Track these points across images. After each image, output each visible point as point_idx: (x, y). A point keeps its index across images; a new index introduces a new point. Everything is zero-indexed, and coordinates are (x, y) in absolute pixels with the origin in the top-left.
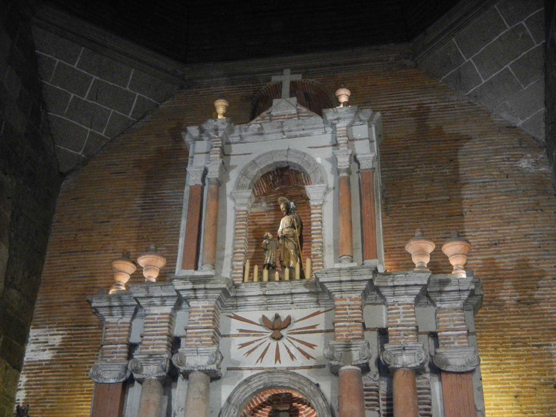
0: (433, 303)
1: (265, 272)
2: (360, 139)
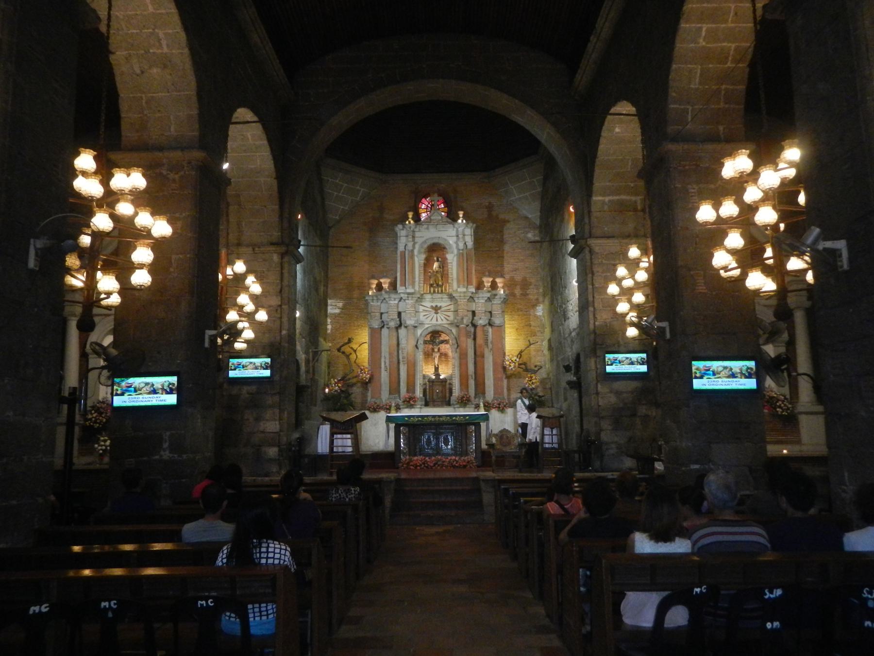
1: (432, 289)
2: (467, 235)
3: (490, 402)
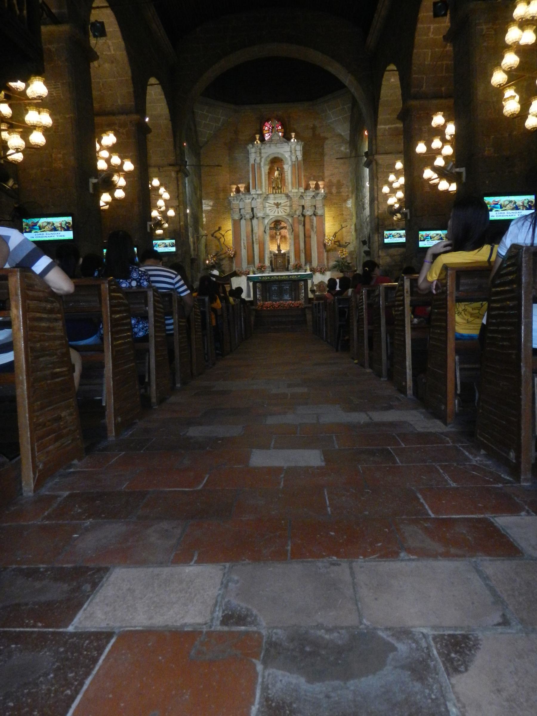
0: (315, 198)
3: (315, 268)
